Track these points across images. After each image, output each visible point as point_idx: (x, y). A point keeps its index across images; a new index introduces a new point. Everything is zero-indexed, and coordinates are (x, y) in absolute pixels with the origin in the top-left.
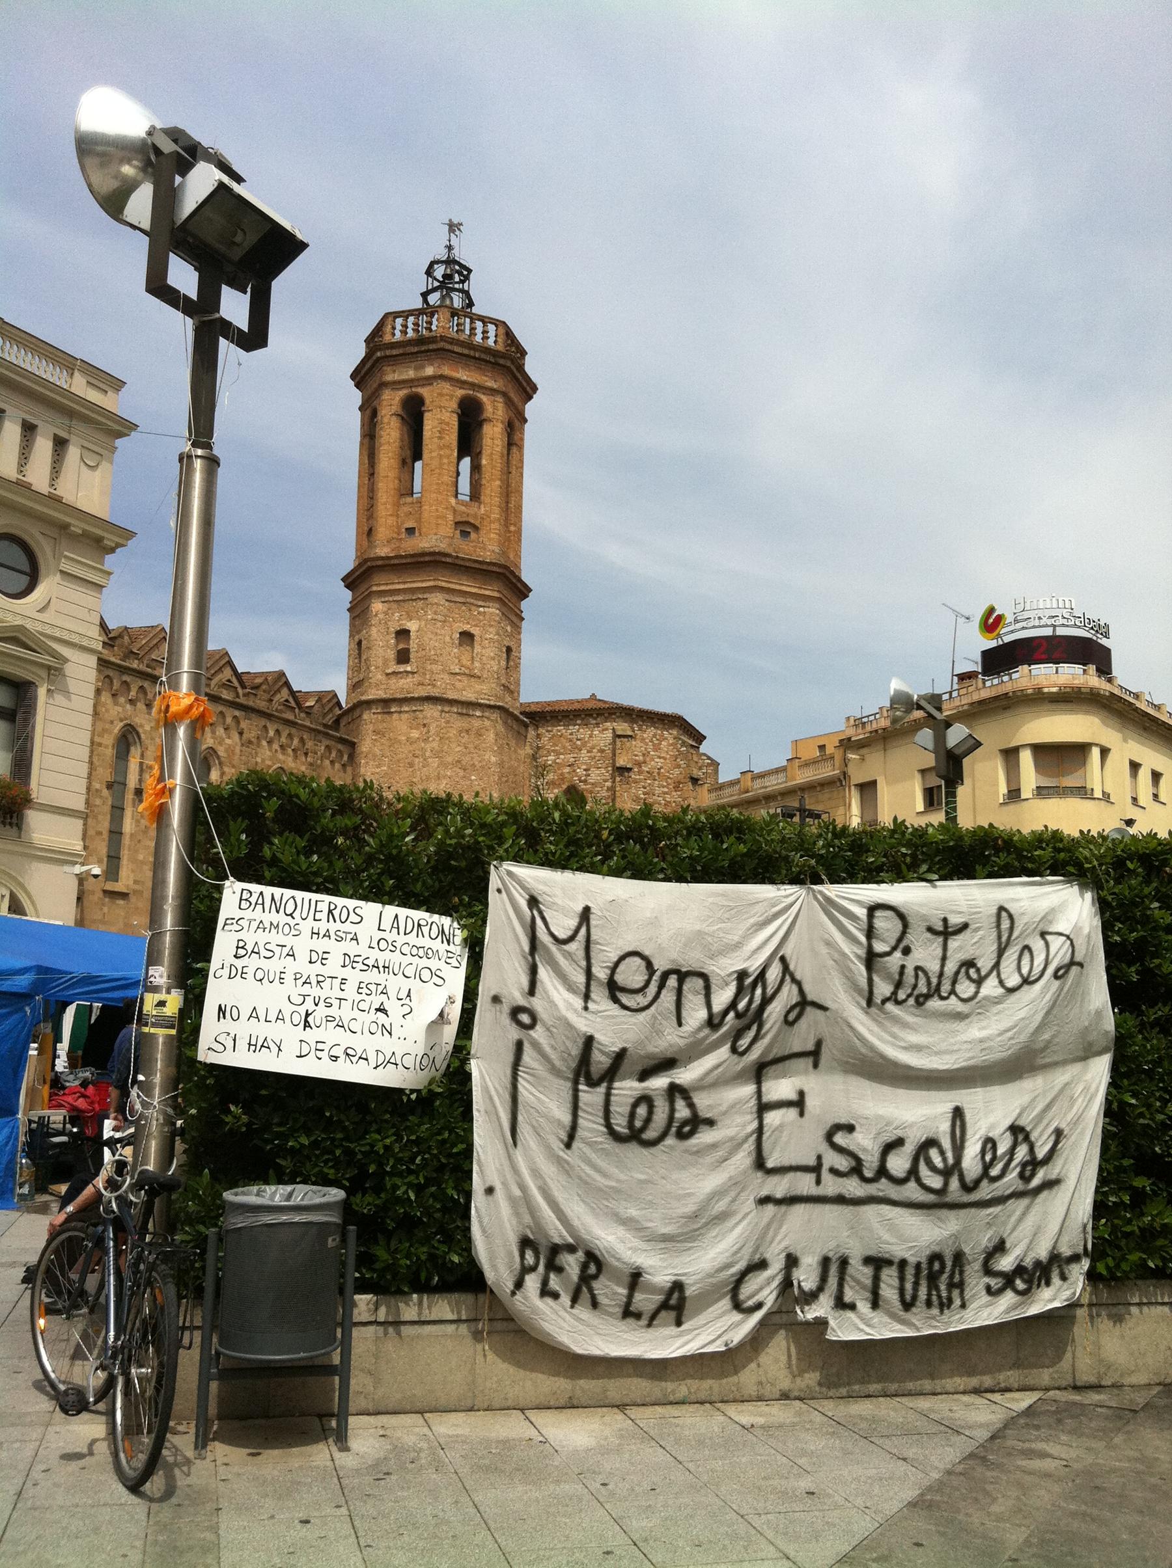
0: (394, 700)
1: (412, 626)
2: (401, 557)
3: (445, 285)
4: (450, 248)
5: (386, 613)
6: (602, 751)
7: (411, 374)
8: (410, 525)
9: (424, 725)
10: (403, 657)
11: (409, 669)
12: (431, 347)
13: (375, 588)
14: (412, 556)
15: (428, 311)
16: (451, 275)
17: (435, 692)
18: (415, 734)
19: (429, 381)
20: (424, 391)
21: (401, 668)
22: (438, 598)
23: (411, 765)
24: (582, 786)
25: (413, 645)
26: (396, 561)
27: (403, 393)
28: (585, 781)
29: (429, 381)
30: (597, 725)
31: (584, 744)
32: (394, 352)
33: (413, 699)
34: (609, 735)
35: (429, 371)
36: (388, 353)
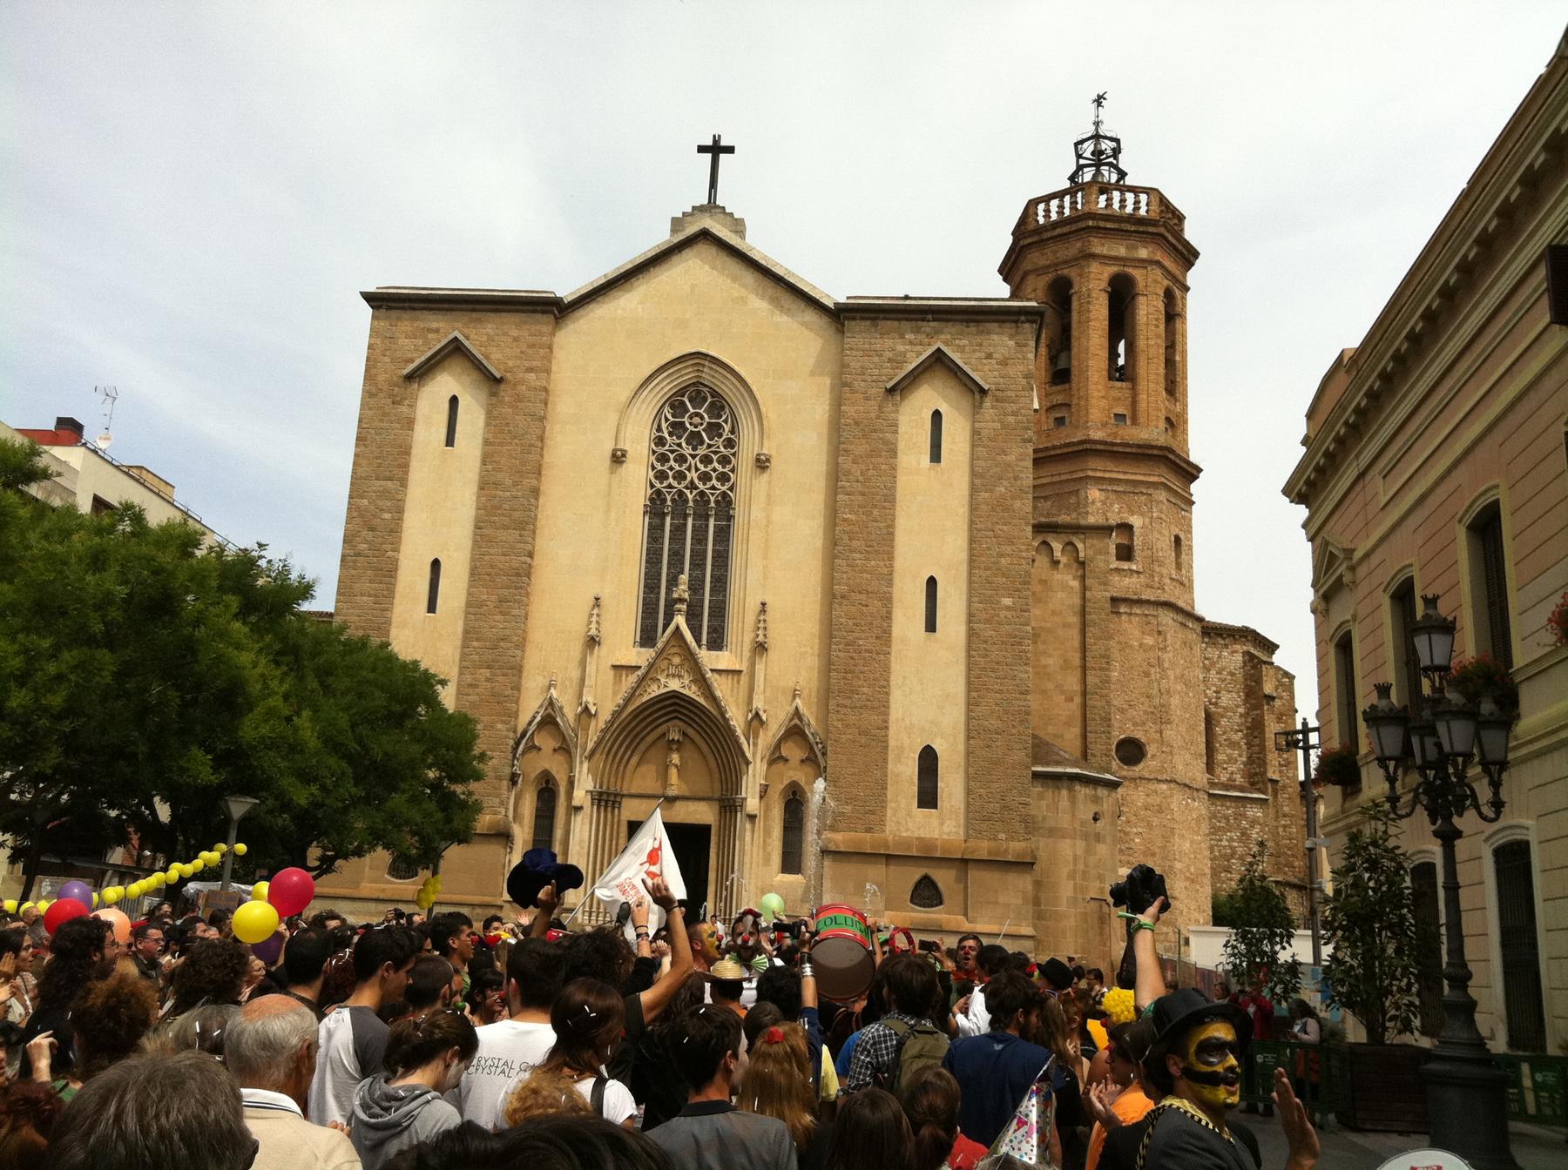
0: (1125, 600)
1: (1136, 521)
2: (1131, 446)
3: (1098, 159)
4: (1097, 124)
5: (1104, 503)
6: (1232, 674)
7: (1122, 251)
8: (1120, 411)
9: (1160, 633)
10: (1125, 553)
11: (1134, 567)
12: (1151, 229)
13: (1090, 473)
14: (1139, 446)
15: (1075, 186)
16: (1100, 153)
17: (1164, 598)
18: (1149, 641)
19: (1143, 263)
20: (1137, 274)
21: (1125, 565)
22: (1162, 495)
23: (1147, 674)
24: (1213, 709)
25: (1138, 542)
26: (1120, 449)
27: (1114, 269)
28: (1216, 704)
29: (1143, 263)
30: (1226, 646)
31: (1213, 664)
32: (1109, 225)
33: (1148, 602)
34: (1239, 658)
35: (1143, 253)
36: (1102, 224)
